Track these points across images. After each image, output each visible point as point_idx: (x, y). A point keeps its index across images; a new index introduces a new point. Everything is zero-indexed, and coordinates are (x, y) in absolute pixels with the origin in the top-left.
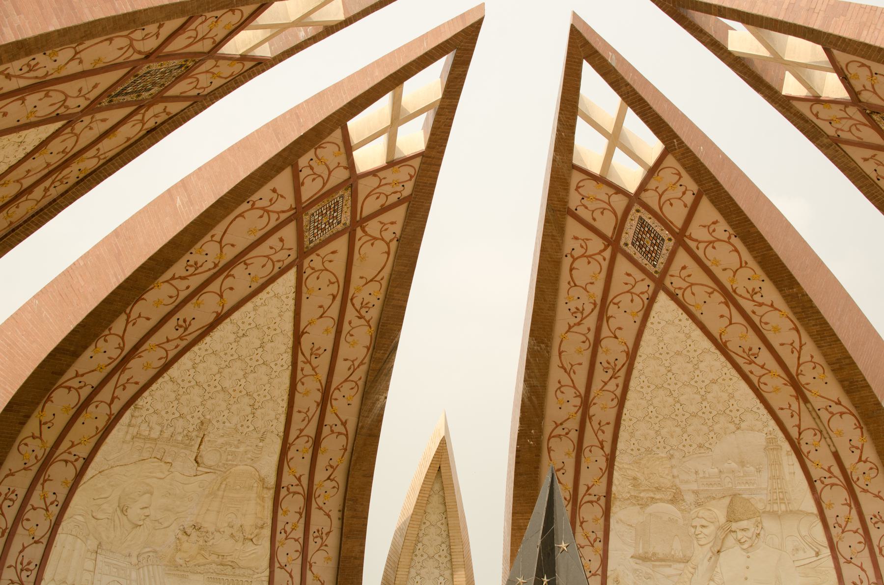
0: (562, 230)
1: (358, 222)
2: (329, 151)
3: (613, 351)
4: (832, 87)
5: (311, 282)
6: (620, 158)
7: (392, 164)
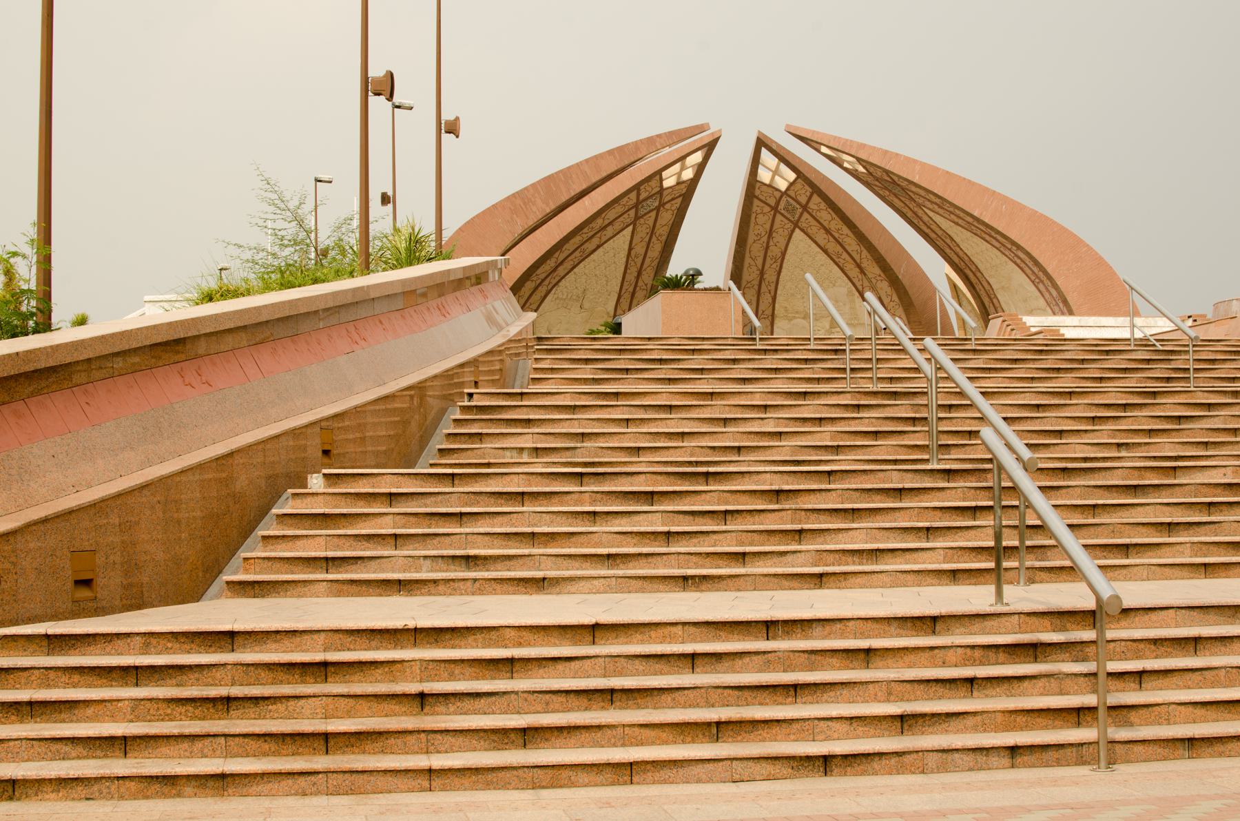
0: (752, 203)
1: (662, 205)
2: (654, 183)
3: (775, 251)
4: (861, 169)
5: (639, 229)
6: (777, 178)
7: (678, 183)
